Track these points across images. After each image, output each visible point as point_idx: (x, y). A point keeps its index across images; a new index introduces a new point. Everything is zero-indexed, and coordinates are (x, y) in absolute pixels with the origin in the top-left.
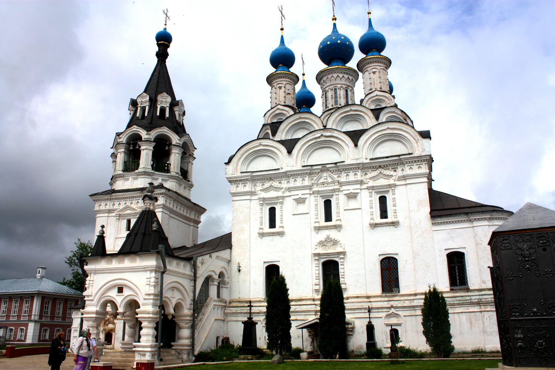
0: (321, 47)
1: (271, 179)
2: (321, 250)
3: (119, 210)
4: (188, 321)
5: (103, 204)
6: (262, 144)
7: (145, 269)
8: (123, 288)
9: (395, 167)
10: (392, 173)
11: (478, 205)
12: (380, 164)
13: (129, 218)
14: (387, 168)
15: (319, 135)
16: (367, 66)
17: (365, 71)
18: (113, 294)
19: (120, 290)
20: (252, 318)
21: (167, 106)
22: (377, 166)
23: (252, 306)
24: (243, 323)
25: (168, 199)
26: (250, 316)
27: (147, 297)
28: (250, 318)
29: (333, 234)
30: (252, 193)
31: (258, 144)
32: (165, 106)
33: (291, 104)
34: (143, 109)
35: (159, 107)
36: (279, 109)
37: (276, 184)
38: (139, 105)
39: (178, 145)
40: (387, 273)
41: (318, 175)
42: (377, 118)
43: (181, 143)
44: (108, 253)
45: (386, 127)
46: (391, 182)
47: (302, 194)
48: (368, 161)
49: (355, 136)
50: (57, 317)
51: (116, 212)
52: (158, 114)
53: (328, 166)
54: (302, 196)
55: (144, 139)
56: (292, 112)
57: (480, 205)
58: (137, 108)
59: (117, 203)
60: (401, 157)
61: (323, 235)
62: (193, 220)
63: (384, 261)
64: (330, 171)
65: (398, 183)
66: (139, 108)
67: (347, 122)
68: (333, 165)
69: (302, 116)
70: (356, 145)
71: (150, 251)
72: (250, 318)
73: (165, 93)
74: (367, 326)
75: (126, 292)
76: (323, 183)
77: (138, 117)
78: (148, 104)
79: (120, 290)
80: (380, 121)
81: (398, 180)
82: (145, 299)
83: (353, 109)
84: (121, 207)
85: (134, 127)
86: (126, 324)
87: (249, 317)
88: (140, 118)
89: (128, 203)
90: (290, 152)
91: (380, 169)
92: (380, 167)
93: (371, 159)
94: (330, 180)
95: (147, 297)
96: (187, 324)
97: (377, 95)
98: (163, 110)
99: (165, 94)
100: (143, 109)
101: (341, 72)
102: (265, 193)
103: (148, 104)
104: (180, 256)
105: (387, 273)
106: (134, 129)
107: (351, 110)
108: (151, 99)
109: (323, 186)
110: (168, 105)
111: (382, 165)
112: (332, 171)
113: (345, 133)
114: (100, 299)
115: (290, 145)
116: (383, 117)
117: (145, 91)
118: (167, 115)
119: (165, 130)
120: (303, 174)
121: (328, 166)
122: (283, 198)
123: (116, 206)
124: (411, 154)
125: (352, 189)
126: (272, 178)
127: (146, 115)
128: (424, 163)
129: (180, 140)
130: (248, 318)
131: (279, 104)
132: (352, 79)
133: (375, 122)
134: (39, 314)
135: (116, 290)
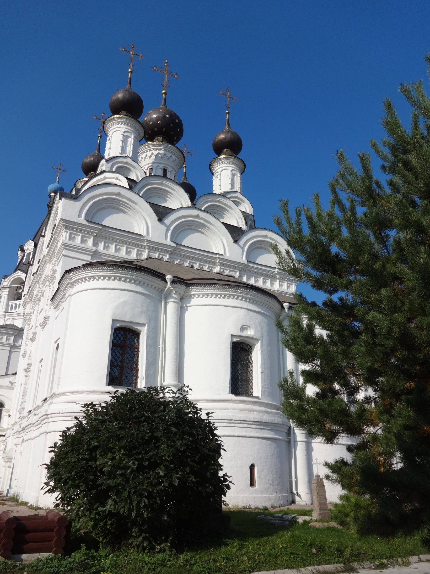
32: (30, 252)
35: (26, 254)
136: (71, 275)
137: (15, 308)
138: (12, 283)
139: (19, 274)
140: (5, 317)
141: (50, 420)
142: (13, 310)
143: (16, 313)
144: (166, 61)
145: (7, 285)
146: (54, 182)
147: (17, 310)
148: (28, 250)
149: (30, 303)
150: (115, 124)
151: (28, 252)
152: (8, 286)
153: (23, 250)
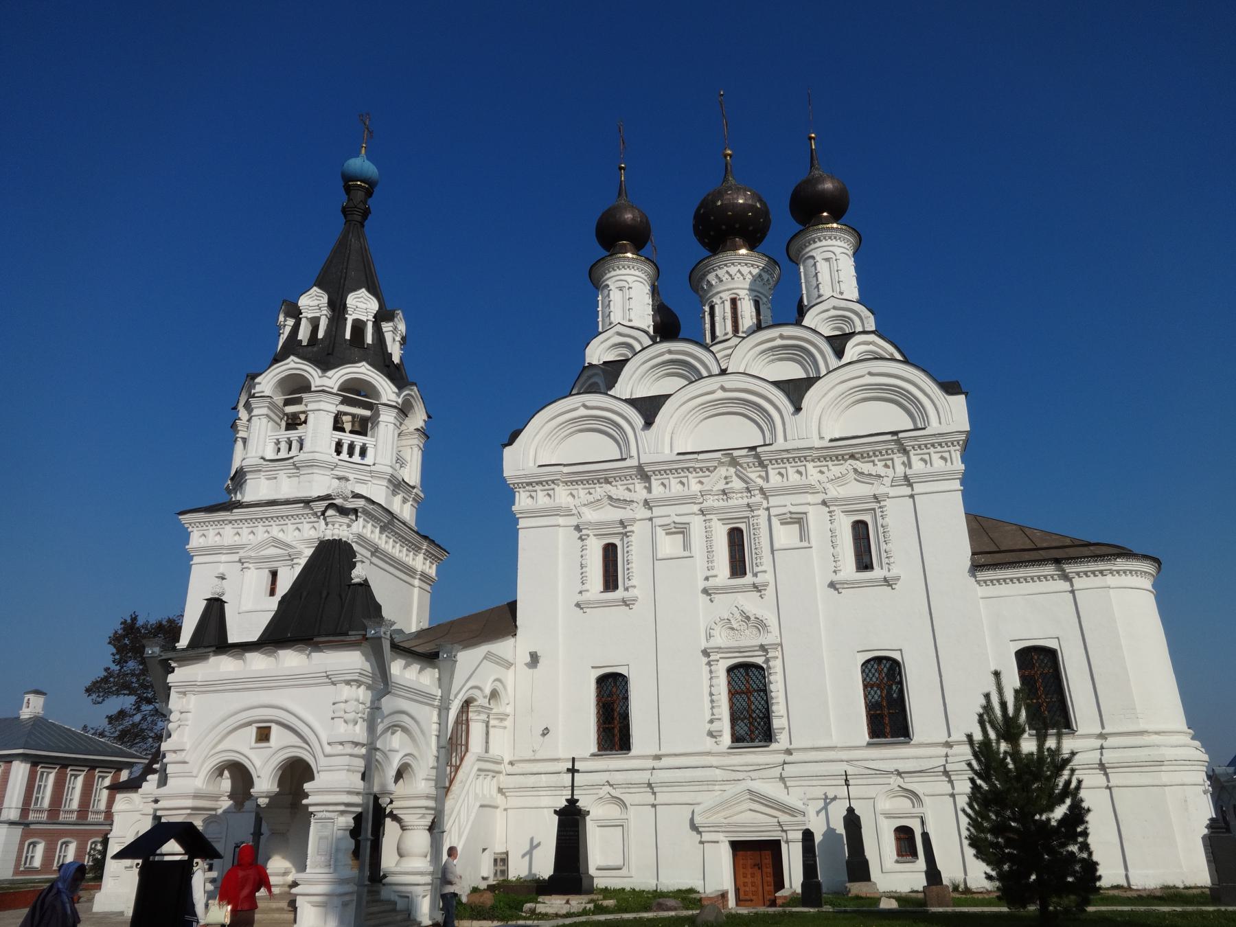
0: (702, 211)
1: (607, 481)
2: (721, 639)
3: (250, 547)
4: (424, 811)
5: (211, 532)
6: (588, 404)
7: (330, 679)
8: (269, 728)
9: (886, 457)
10: (879, 469)
11: (1077, 543)
12: (854, 451)
13: (274, 565)
14: (866, 459)
16: (813, 246)
17: (806, 256)
18: (243, 746)
19: (263, 735)
20: (577, 801)
21: (367, 320)
22: (846, 454)
23: (578, 771)
24: (556, 812)
25: (367, 522)
26: (573, 794)
28: (572, 802)
29: (751, 604)
30: (568, 513)
32: (364, 319)
33: (644, 327)
34: (315, 323)
36: (619, 334)
37: (618, 491)
38: (304, 315)
39: (394, 404)
40: (876, 693)
41: (711, 472)
42: (839, 353)
43: (400, 401)
44: (230, 641)
45: (865, 371)
46: (879, 489)
47: (676, 515)
48: (826, 443)
49: (795, 391)
50: (66, 812)
51: (241, 551)
52: (348, 336)
53: (736, 453)
54: (678, 519)
55: (316, 387)
56: (647, 341)
57: (1082, 543)
58: (301, 319)
59: (245, 531)
60: (901, 435)
61: (724, 605)
62: (421, 575)
63: (869, 666)
64: (742, 467)
65: (893, 492)
66: (304, 322)
67: (773, 361)
69: (672, 349)
70: (798, 409)
71: (347, 634)
72: (572, 802)
73: (363, 290)
74: (845, 818)
75: (278, 736)
76: (723, 491)
77: (301, 341)
78: (325, 312)
79: (263, 735)
80: (846, 359)
81: (892, 486)
83: (785, 333)
85: (293, 360)
86: (263, 822)
87: (569, 797)
88: (305, 343)
89: (275, 531)
90: (649, 423)
91: (850, 461)
92: (852, 456)
93: (831, 440)
94: (737, 484)
96: (423, 816)
97: (834, 308)
98: (359, 327)
99: (363, 292)
100: (315, 323)
101: (746, 264)
102: (594, 510)
103: (325, 312)
104: (412, 649)
105: (876, 693)
106: (292, 365)
107: (782, 337)
108: (331, 304)
109: (725, 497)
110: (371, 318)
111: (857, 453)
112: (745, 465)
113: (776, 384)
114: (206, 758)
115: (649, 408)
116: (852, 350)
118: (369, 339)
119: (363, 371)
120: (679, 471)
121: (736, 453)
122: (634, 520)
124: (924, 429)
125: (787, 504)
126: (610, 480)
127: (321, 335)
128: (952, 448)
129: (398, 395)
130: (567, 800)
131: (619, 323)
132: (768, 280)
133: (833, 362)
134: (20, 806)
135: (252, 731)
136: (1118, 560)
137: (351, 454)
138: (340, 390)
139: (363, 370)
140: (332, 470)
141: (1163, 768)
142: (344, 455)
143: (373, 468)
144: (722, 93)
145: (333, 388)
146: (357, 155)
147: (356, 458)
148: (355, 310)
149: (561, 484)
150: (842, 239)
151: (355, 316)
152: (335, 391)
153: (338, 308)
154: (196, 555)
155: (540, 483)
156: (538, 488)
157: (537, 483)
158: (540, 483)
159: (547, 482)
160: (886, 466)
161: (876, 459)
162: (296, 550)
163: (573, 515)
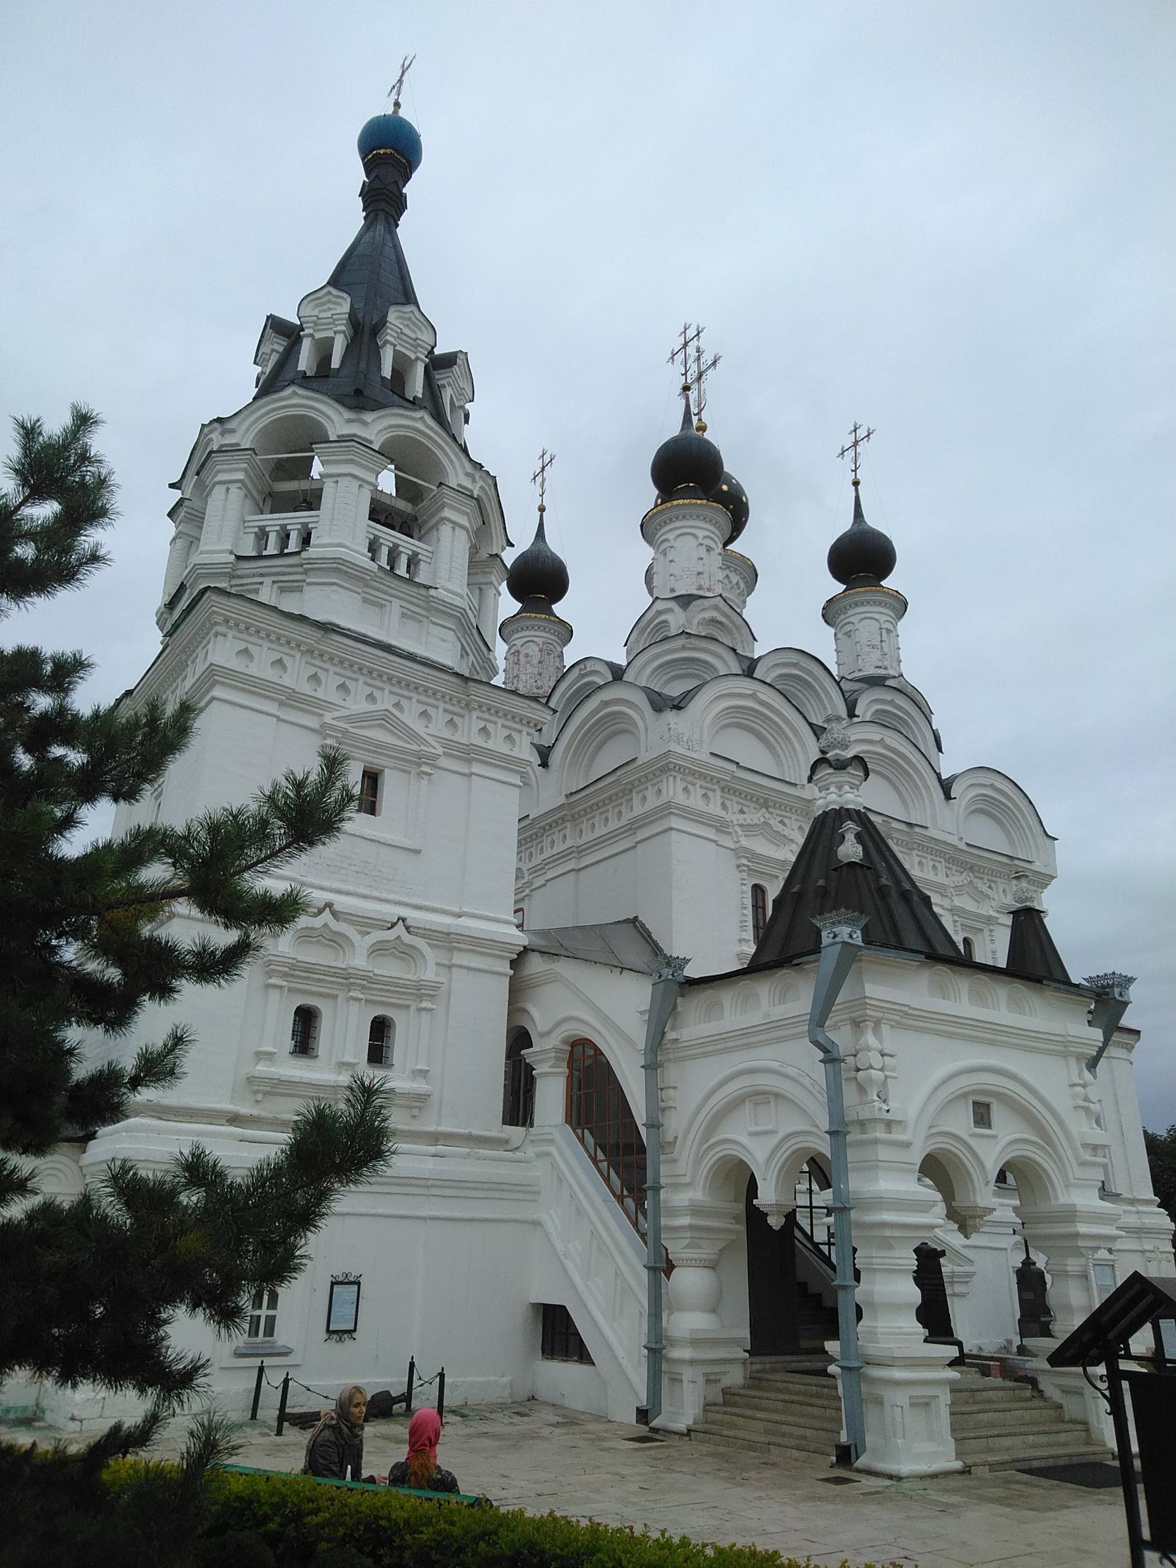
1: (766, 805)
3: (346, 713)
15: (877, 737)
19: (982, 1114)
27: (1087, 1157)
31: (751, 692)
59: (331, 680)
68: (903, 827)
79: (982, 1114)
82: (1083, 1164)
84: (357, 704)
92: (971, 869)
95: (1087, 1157)
117: (338, 280)
121: (895, 825)
123: (327, 691)
154: (222, 684)
155: (705, 777)
156: (699, 783)
157: (701, 774)
158: (705, 777)
159: (712, 778)
160: (990, 887)
161: (986, 877)
162: (434, 751)
163: (730, 833)
